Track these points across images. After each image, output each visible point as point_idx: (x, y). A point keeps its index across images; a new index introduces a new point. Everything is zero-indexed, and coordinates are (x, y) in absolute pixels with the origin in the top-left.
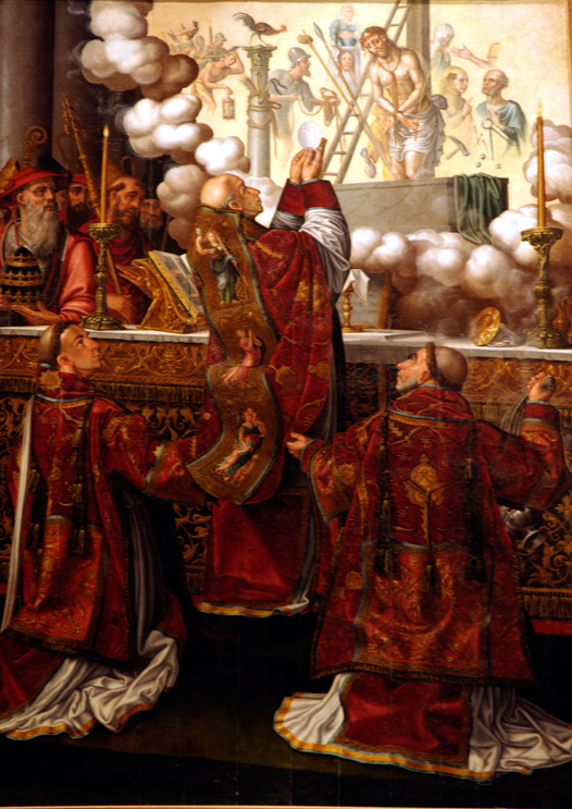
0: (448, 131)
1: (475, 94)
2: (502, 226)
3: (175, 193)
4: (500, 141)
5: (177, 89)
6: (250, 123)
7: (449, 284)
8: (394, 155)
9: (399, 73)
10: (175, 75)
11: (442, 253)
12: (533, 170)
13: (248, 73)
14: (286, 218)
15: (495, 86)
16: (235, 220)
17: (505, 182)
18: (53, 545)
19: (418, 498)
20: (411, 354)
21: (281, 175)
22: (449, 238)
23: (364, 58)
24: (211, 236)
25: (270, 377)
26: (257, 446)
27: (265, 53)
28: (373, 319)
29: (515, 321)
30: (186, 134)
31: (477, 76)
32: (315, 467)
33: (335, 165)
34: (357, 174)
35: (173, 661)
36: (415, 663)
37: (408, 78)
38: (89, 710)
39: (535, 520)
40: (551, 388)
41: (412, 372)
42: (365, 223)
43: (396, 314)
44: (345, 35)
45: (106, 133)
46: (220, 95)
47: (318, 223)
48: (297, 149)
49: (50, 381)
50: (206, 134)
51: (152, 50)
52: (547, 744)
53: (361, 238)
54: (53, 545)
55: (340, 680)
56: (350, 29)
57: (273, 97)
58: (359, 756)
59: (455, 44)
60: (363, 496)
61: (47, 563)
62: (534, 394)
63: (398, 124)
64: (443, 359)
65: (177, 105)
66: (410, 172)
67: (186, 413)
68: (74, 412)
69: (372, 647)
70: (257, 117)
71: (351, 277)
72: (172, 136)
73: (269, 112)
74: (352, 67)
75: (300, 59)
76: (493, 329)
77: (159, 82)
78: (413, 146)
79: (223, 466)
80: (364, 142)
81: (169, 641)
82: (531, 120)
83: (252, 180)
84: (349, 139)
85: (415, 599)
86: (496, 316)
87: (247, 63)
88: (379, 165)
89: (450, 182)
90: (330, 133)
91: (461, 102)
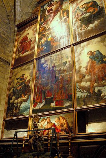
2: (67, 65)
11: (62, 68)
16: (49, 70)
19: (60, 86)
20: (60, 76)
22: (63, 67)
30: (47, 65)
32: (54, 86)
34: (57, 64)
39: (69, 86)
47: (54, 69)
50: (48, 65)
53: (57, 69)
55: (55, 101)
58: (56, 107)
62: (69, 76)
72: (46, 66)
73: (51, 62)
75: (53, 58)
83: (50, 67)
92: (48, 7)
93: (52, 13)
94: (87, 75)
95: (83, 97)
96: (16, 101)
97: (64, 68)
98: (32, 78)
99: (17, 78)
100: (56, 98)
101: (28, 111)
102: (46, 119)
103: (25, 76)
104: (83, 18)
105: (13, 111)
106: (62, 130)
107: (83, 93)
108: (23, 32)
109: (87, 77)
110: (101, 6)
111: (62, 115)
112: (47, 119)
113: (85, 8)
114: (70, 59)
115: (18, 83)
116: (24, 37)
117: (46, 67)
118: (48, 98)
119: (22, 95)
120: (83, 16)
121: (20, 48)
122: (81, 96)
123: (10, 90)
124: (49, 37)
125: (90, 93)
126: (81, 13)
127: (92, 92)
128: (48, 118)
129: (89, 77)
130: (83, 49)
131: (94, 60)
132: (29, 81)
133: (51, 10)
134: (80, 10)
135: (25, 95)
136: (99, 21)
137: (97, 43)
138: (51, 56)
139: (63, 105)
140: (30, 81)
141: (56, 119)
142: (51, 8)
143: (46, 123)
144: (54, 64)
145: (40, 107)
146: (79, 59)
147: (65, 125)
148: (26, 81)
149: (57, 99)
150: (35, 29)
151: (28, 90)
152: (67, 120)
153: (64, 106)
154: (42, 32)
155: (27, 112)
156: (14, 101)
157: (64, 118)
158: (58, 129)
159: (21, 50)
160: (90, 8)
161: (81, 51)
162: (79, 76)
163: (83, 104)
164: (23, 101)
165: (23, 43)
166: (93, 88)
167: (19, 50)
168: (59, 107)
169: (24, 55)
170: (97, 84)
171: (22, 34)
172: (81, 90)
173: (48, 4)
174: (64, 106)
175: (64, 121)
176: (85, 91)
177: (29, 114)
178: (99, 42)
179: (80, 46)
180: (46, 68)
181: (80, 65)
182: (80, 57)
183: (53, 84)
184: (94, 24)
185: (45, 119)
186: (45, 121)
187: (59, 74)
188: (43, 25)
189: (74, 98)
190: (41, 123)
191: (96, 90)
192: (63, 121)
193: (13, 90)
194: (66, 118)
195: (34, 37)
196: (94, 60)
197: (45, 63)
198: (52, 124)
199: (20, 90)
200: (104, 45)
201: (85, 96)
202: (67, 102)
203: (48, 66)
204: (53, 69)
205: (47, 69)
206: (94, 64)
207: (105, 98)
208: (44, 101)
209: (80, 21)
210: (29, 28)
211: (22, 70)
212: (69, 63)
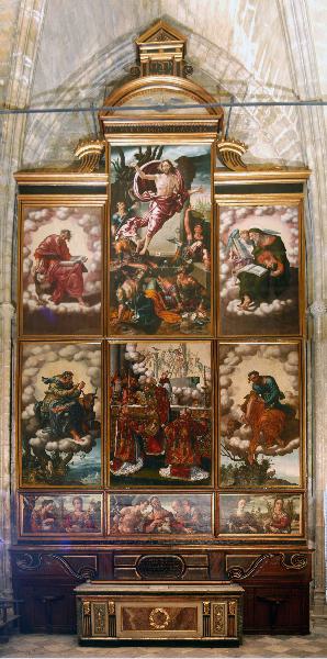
1: (194, 362)
2: (198, 386)
16: (152, 385)
21: (160, 377)
29: (200, 403)
34: (173, 376)
41: (182, 412)
47: (166, 386)
53: (174, 388)
65: (142, 364)
72: (141, 370)
73: (158, 366)
98: (99, 391)
105: (43, 468)
109: (243, 430)
114: (208, 376)
115: (53, 393)
117: (143, 374)
122: (230, 466)
123: (23, 409)
124: (147, 284)
125: (247, 462)
129: (248, 430)
130: (240, 361)
135: (81, 434)
138: (156, 345)
146: (230, 382)
148: (81, 396)
156: (43, 444)
169: (62, 307)
176: (238, 458)
182: (232, 378)
191: (260, 459)
193: (37, 410)
200: (285, 369)
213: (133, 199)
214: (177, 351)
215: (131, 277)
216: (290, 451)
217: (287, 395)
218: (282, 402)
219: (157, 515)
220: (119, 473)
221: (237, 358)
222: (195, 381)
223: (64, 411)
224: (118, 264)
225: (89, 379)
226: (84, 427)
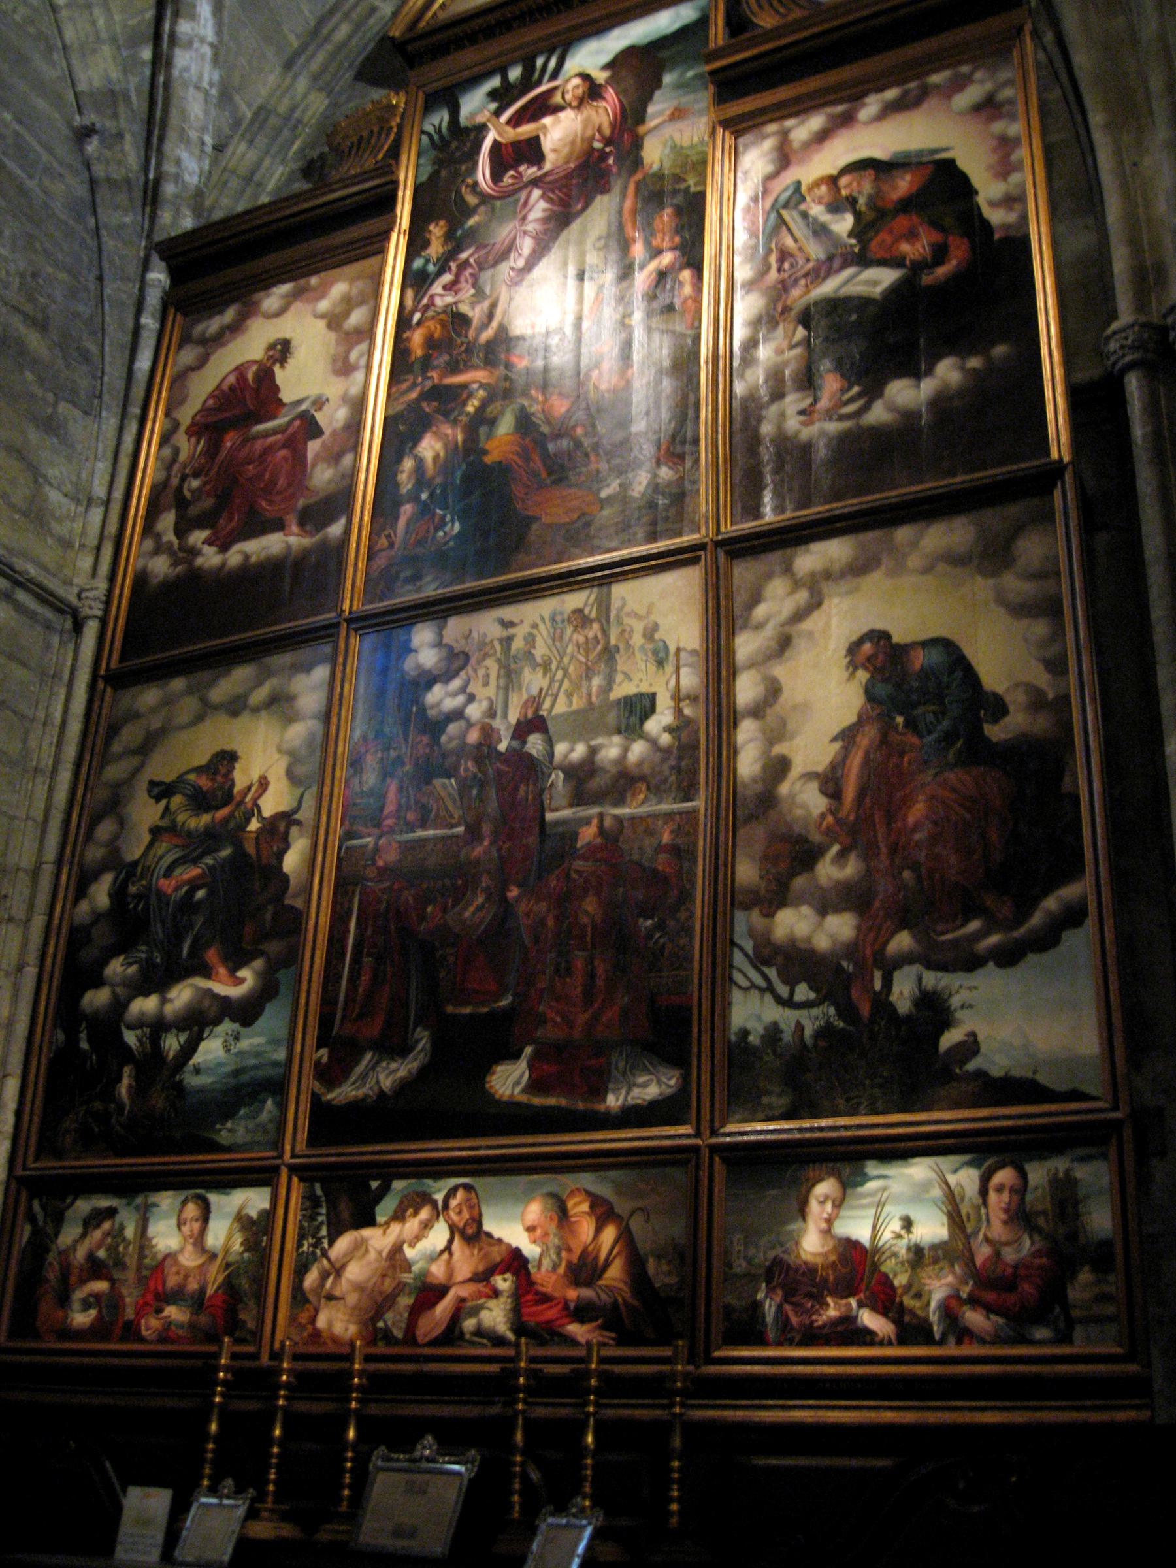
0: (619, 668)
1: (637, 640)
2: (653, 726)
3: (451, 739)
4: (652, 667)
5: (456, 674)
6: (498, 687)
7: (614, 770)
8: (584, 690)
9: (591, 635)
10: (456, 665)
11: (610, 750)
12: (673, 682)
13: (498, 654)
14: (515, 744)
15: (650, 633)
16: (485, 750)
17: (654, 695)
18: (365, 978)
19: (585, 920)
20: (587, 821)
21: (513, 717)
22: (617, 739)
23: (569, 630)
24: (470, 764)
25: (499, 850)
26: (488, 899)
27: (509, 639)
28: (564, 802)
29: (657, 789)
30: (460, 699)
31: (638, 627)
32: (522, 908)
33: (547, 704)
34: (561, 707)
35: (428, 1047)
36: (577, 1034)
37: (596, 637)
38: (378, 1082)
39: (661, 926)
40: (677, 832)
41: (588, 834)
42: (563, 738)
43: (579, 798)
44: (558, 618)
45: (414, 709)
46: (481, 672)
47: (535, 744)
48: (525, 697)
49: (371, 873)
50: (471, 698)
51: (444, 652)
52: (659, 1082)
53: (560, 748)
54: (365, 978)
55: (528, 1050)
56: (561, 613)
57: (513, 666)
58: (537, 1101)
59: (627, 609)
60: (551, 923)
61: (361, 990)
62: (666, 838)
63: (588, 669)
64: (608, 822)
65: (456, 684)
66: (594, 699)
67: (447, 882)
68: (383, 890)
69: (550, 1025)
70: (502, 682)
71: (553, 776)
72: (450, 704)
73: (510, 677)
74: (561, 637)
75: (530, 640)
76: (642, 796)
77: (447, 672)
78: (596, 682)
79: (467, 914)
80: (566, 682)
81: (427, 1033)
82: (672, 649)
83: (497, 723)
84: (556, 685)
85: (579, 989)
86: (644, 787)
87: (498, 647)
88: (575, 699)
89: (618, 701)
90: (545, 683)
91: (628, 646)
92: (498, 113)
93: (535, 182)
94: (836, 848)
95: (787, 1037)
96: (146, 1005)
97: (626, 750)
98: (309, 802)
99: (152, 784)
100: (542, 1020)
101: (264, 1116)
102: (439, 1197)
103: (242, 777)
104: (834, 305)
105: (109, 1093)
106: (582, 1313)
107: (788, 1003)
108: (229, 315)
110: (1007, 227)
111: (587, 1180)
112: (454, 1203)
113: (858, 215)
114: (690, 679)
115: (173, 829)
116: (240, 370)
117: (458, 715)
118: (468, 1010)
119: (212, 955)
120: (828, 288)
121: (195, 483)
122: (773, 1033)
123: (81, 892)
124: (492, 422)
125: (847, 1011)
126: (816, 251)
127: (865, 1010)
128: (460, 1194)
129: (851, 869)
130: (815, 604)
131: (900, 720)
132: (282, 827)
133: (531, 151)
134: (805, 215)
135: (236, 960)
136: (974, 362)
137: (941, 567)
138: (508, 612)
139: (599, 1093)
140: (294, 830)
141: (535, 1210)
142: (526, 130)
143: (439, 1236)
144: (535, 702)
145: (387, 1083)
146: (774, 691)
147: (615, 1272)
148: (254, 825)
149: (549, 1033)
150: (357, 317)
151: (268, 916)
152: (636, 1224)
153: (613, 1101)
154: (426, 363)
155: (251, 1124)
156: (119, 1006)
157: (603, 1212)
158: (545, 1298)
159: (208, 503)
160: (902, 222)
161: (799, 616)
162: (759, 847)
163: (781, 1102)
164: (213, 1011)
165: (230, 440)
166: (878, 976)
167: (181, 504)
168: (563, 1102)
169: (234, 557)
170: (914, 937)
171: (219, 339)
172: (772, 973)
173: (495, 82)
174: (613, 1101)
175: (609, 1234)
176: (803, 992)
177: (278, 1145)
178: (956, 560)
179: (788, 570)
180: (453, 728)
181: (778, 749)
182: (779, 671)
183: (514, 892)
184: (927, 387)
185: (425, 1199)
186: (425, 1213)
187: (579, 798)
188: (437, 288)
189: (706, 1038)
190: (395, 1228)
192: (598, 1230)
193: (118, 894)
194: (622, 1207)
195: (345, 399)
196: (900, 720)
197: (446, 676)
198: (497, 1255)
199: (187, 905)
200: (1001, 599)
201: (808, 1032)
202: (635, 1067)
203: (474, 711)
204: (524, 743)
205: (463, 736)
206: (901, 754)
207: (971, 1066)
208: (423, 1039)
209: (801, 332)
210: (296, 295)
211: (207, 709)
212: (678, 712)
213: (472, 200)
214: (580, 618)
215: (446, 414)
216: (1046, 940)
217: (1016, 700)
218: (995, 732)
219: (465, 1262)
220: (345, 1093)
221: (802, 596)
222: (643, 706)
223: (194, 886)
224: (414, 385)
225: (281, 764)
226: (249, 929)
